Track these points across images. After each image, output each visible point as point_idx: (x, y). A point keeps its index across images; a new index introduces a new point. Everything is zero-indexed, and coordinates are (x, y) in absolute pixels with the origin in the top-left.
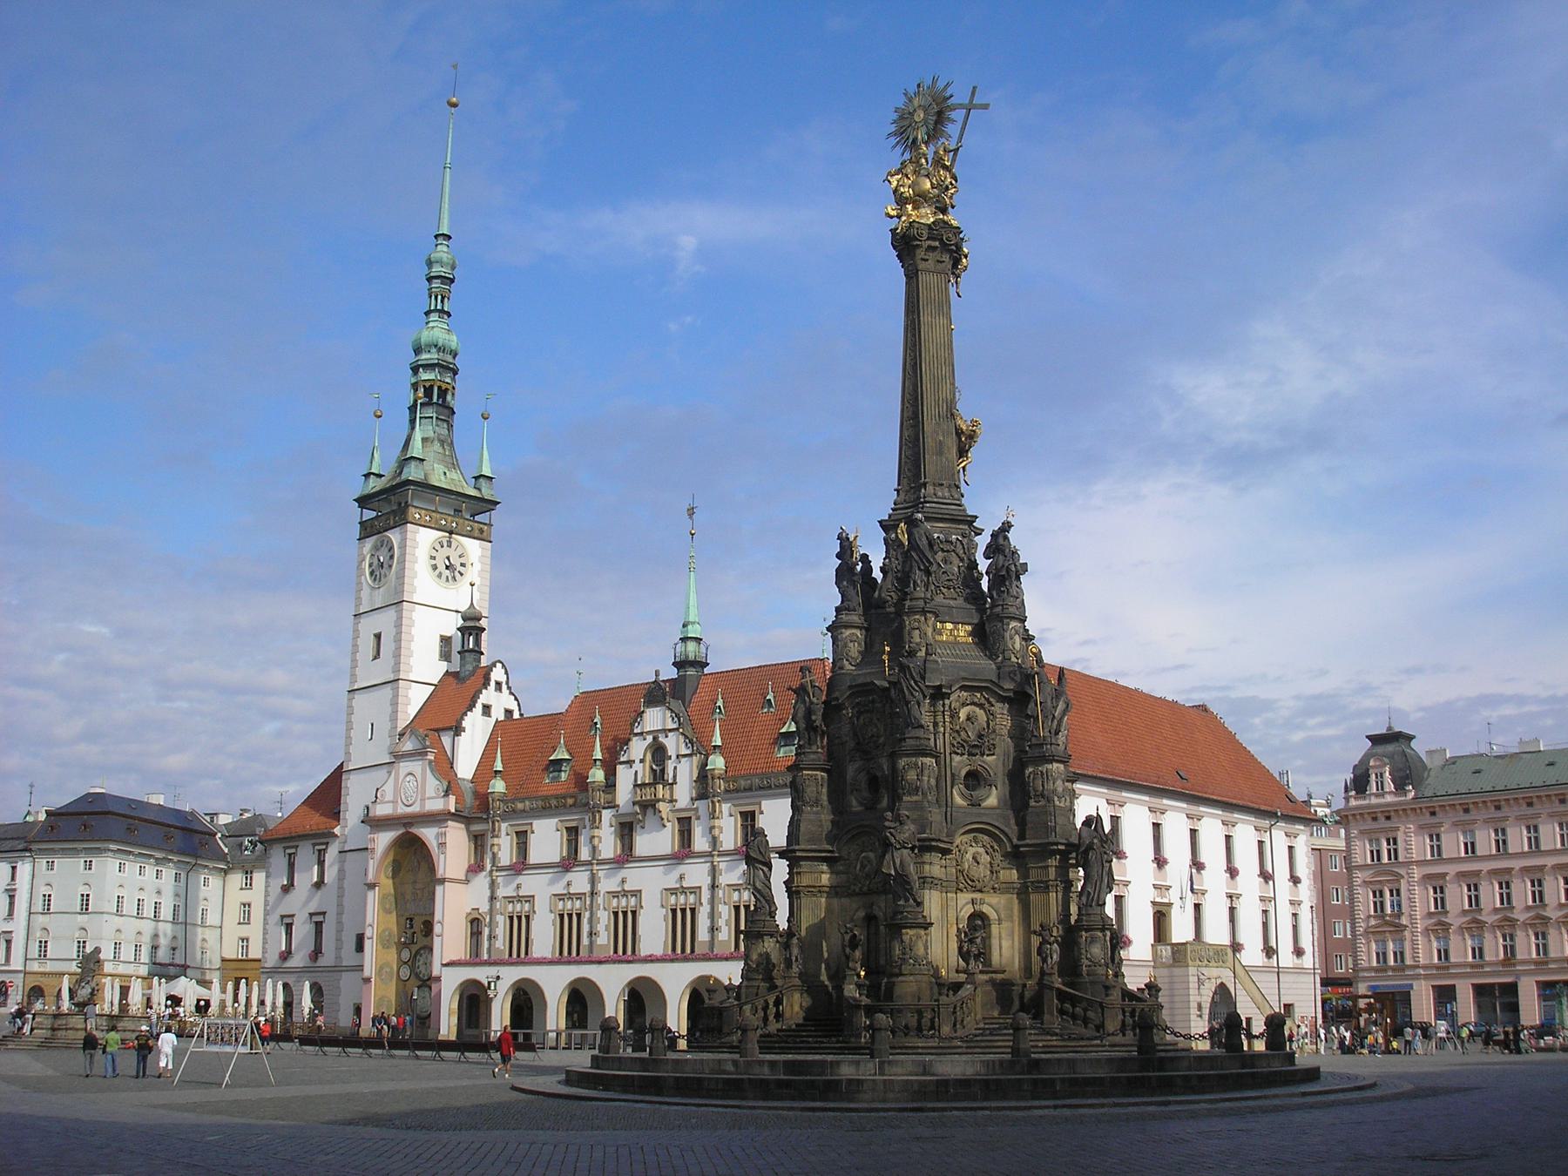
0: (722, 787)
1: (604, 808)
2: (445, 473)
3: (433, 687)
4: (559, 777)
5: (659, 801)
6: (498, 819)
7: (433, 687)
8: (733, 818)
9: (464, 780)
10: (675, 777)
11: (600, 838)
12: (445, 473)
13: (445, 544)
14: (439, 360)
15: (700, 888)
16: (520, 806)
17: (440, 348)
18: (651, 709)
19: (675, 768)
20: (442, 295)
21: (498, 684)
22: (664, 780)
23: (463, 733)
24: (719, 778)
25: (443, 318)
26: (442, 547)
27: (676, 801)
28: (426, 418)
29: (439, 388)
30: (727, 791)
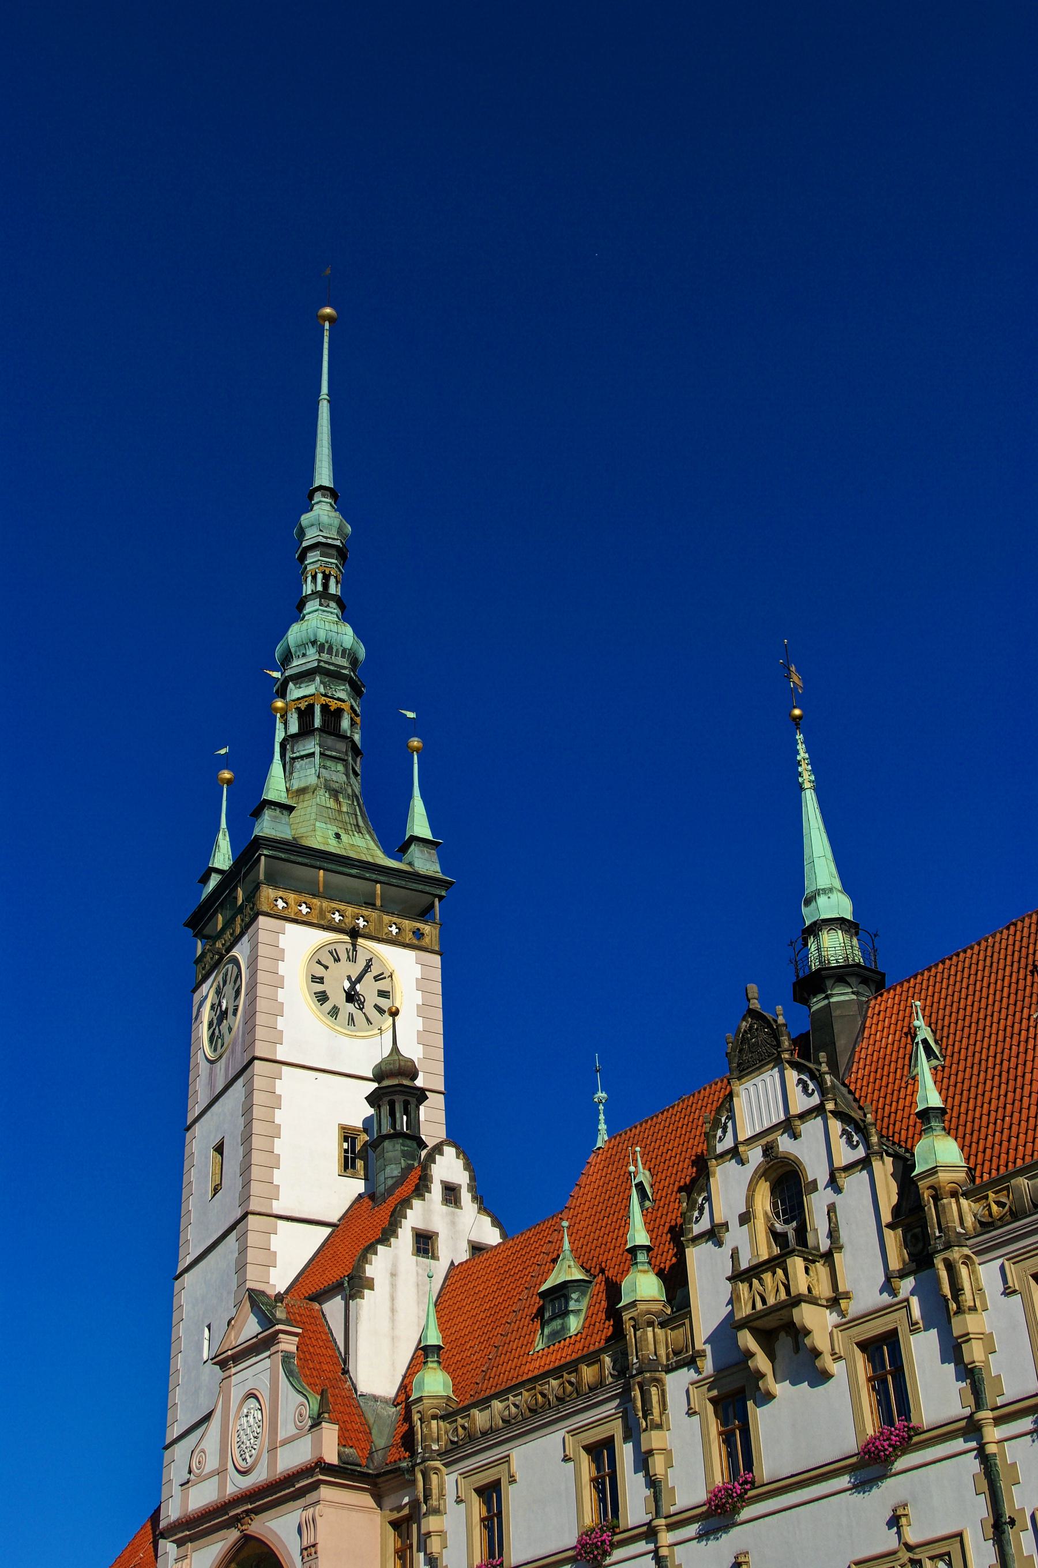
0: (969, 1220)
1: (669, 1370)
2: (338, 836)
3: (329, 1230)
4: (564, 1328)
5: (796, 1301)
6: (437, 1464)
7: (329, 1230)
8: (1017, 1298)
9: (375, 1398)
10: (833, 1234)
11: (667, 1453)
12: (338, 836)
13: (343, 956)
14: (319, 661)
15: (960, 1535)
16: (480, 1418)
17: (322, 646)
18: (749, 1085)
19: (832, 1209)
20: (324, 573)
21: (451, 1193)
22: (805, 1245)
23: (366, 1292)
24: (954, 1194)
25: (328, 606)
26: (337, 960)
27: (847, 1296)
28: (302, 757)
29: (325, 708)
30: (985, 1225)
